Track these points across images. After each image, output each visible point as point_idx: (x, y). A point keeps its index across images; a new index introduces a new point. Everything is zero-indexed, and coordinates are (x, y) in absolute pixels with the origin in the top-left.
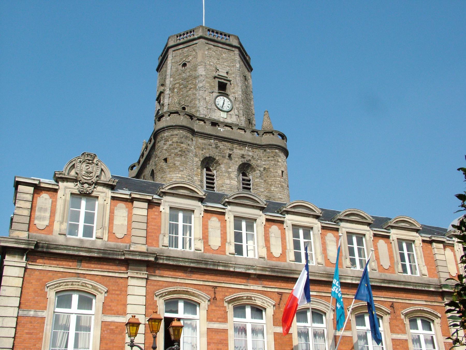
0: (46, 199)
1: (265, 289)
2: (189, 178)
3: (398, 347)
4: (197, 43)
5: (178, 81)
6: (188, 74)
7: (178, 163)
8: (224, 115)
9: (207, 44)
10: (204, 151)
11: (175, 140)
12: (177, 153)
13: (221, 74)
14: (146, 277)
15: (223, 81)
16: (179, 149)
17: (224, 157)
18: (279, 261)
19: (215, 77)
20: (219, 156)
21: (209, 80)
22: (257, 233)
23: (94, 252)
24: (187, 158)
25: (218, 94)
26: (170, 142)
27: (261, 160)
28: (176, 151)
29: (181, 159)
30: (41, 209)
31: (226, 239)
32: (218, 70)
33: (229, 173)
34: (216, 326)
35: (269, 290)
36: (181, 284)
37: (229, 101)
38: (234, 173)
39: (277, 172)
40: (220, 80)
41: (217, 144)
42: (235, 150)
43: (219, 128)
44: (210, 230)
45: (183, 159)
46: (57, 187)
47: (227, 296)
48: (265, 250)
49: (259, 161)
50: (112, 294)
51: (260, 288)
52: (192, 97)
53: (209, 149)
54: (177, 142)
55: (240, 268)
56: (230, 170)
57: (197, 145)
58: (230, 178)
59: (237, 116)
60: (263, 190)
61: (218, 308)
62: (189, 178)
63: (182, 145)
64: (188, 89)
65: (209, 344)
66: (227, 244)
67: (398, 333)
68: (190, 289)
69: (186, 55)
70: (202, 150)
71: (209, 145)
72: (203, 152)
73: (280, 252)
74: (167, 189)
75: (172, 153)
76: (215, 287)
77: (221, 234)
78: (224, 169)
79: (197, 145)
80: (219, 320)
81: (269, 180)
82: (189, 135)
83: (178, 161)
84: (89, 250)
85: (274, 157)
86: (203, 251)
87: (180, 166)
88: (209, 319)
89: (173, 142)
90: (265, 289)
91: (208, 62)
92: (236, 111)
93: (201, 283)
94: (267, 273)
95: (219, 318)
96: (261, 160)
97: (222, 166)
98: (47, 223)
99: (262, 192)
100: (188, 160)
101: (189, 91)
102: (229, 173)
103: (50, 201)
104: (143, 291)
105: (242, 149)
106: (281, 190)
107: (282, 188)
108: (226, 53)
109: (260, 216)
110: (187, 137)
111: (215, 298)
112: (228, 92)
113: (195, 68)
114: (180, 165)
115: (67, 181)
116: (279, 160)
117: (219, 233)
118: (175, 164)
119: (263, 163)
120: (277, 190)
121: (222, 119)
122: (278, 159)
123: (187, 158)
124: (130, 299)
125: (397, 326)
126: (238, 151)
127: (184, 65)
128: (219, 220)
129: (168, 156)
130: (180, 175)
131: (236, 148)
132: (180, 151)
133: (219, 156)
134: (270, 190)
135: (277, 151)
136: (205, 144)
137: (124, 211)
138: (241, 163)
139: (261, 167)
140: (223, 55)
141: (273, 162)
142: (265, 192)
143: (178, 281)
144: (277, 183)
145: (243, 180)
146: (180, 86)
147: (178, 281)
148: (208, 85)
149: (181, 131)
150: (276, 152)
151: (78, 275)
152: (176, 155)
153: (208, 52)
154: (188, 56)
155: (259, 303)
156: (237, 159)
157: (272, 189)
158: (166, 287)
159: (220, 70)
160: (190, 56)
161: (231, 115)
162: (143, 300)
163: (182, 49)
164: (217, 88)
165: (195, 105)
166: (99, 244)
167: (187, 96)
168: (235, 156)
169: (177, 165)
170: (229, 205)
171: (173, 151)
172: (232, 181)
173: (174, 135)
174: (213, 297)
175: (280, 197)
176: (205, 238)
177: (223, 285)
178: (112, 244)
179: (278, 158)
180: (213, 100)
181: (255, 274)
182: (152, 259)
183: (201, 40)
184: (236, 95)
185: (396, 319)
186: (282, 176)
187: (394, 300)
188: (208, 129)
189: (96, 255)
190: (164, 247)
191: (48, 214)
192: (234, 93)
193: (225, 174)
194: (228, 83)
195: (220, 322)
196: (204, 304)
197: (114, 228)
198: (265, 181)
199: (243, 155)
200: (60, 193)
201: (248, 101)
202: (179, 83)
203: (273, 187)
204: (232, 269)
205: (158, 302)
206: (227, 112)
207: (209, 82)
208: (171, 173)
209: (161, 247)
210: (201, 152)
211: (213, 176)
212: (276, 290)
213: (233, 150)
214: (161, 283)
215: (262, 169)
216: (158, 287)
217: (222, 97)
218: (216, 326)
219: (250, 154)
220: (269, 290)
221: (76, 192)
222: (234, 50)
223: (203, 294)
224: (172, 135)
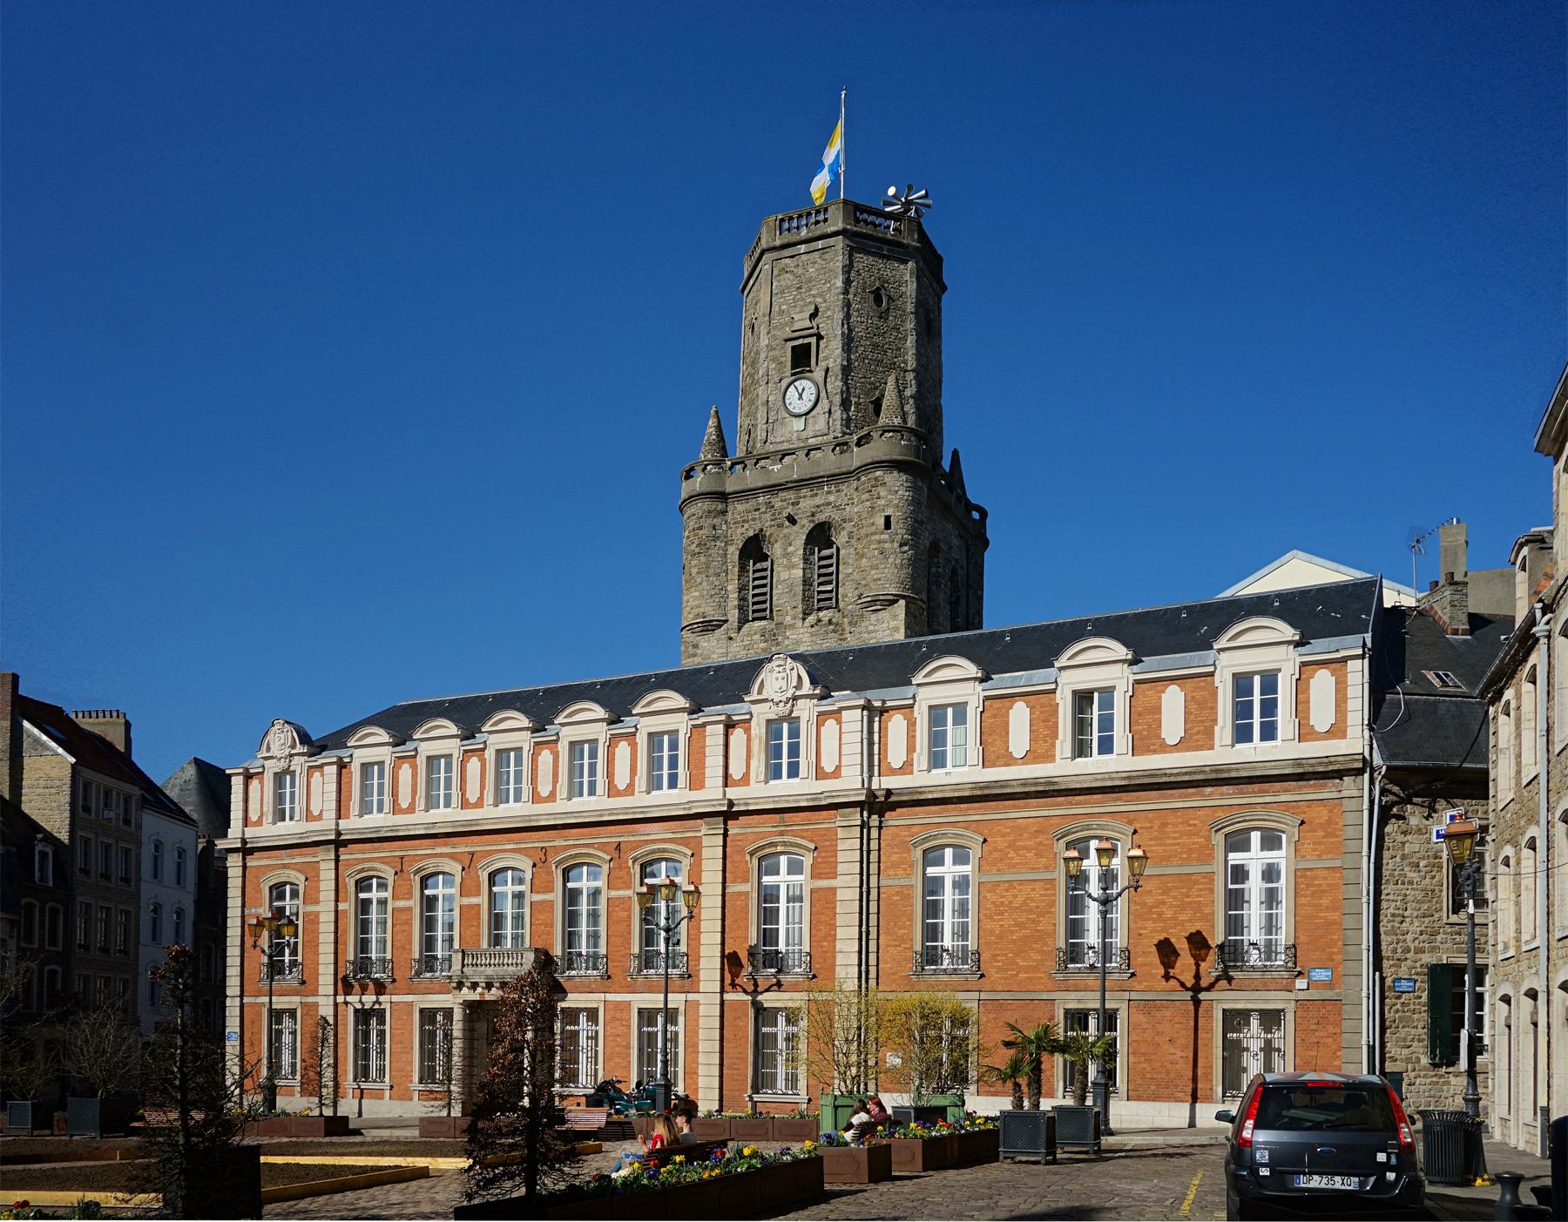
8: (798, 424)
10: (746, 526)
24: (710, 555)
54: (694, 530)
56: (790, 549)
60: (850, 571)
67: (619, 889)
70: (743, 526)
71: (755, 510)
76: (402, 858)
96: (853, 503)
105: (816, 495)
114: (697, 573)
122: (878, 494)
125: (621, 878)
126: (807, 504)
130: (697, 594)
131: (805, 497)
133: (771, 526)
135: (878, 473)
144: (872, 547)
150: (876, 479)
151: (285, 866)
175: (876, 577)
179: (879, 489)
185: (620, 868)
187: (622, 839)
223: (388, 868)
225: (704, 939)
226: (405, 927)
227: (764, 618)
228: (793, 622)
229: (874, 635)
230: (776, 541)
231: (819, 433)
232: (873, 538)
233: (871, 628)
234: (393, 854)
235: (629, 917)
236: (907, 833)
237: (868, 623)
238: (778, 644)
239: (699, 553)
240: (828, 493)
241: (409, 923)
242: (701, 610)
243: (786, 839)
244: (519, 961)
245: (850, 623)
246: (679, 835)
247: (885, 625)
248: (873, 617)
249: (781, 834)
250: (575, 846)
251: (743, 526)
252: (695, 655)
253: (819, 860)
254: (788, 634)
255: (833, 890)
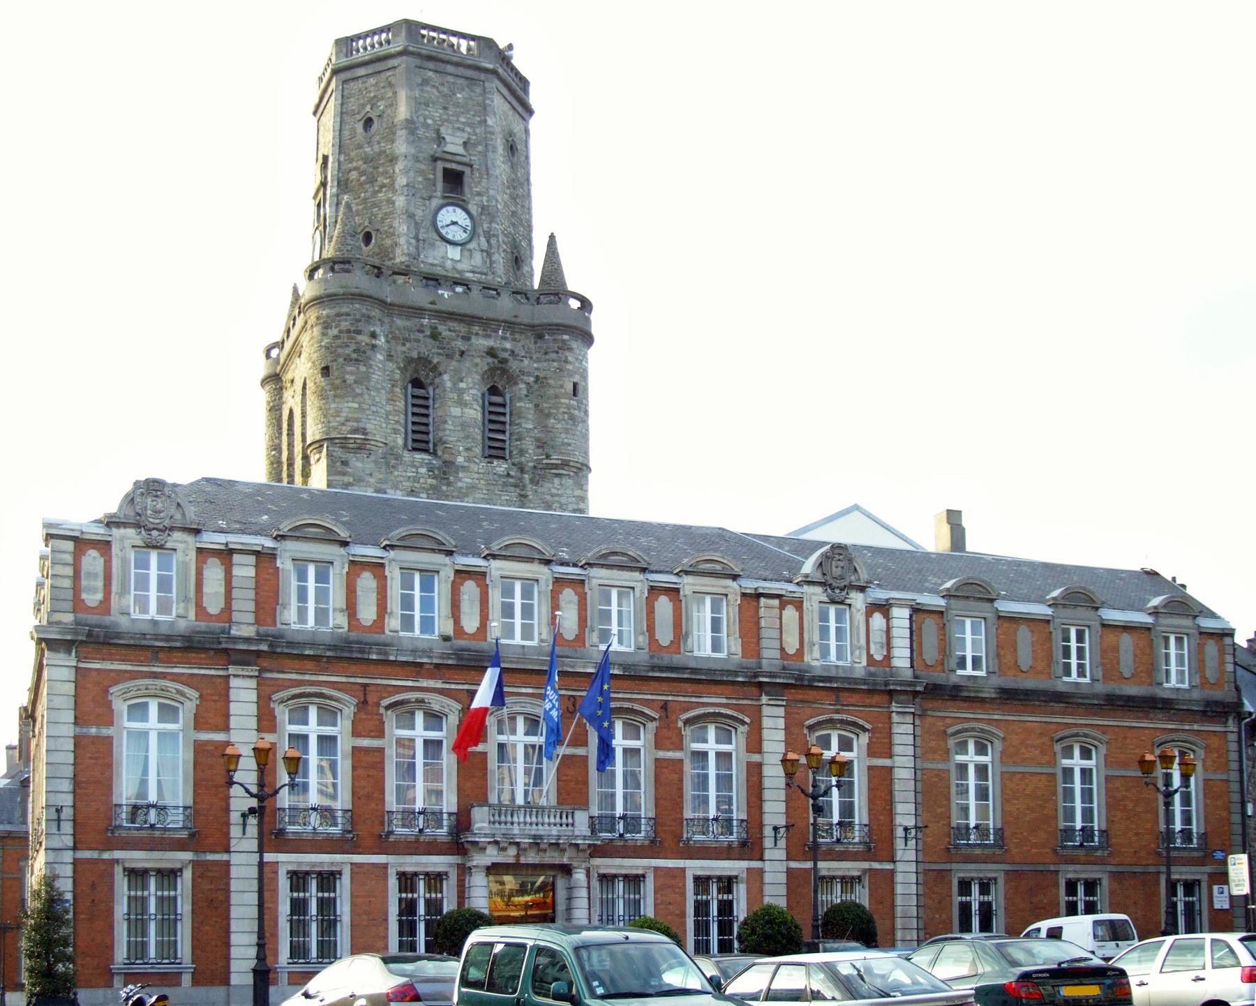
0: (95, 558)
1: (447, 686)
2: (374, 409)
3: (664, 770)
4: (394, 68)
5: (355, 164)
6: (376, 148)
7: (350, 379)
8: (454, 253)
9: (420, 67)
10: (408, 345)
11: (345, 325)
12: (349, 355)
13: (450, 148)
14: (257, 674)
15: (454, 166)
16: (353, 347)
17: (449, 356)
18: (474, 639)
19: (435, 159)
20: (440, 354)
21: (423, 167)
22: (439, 594)
23: (176, 641)
25: (441, 201)
26: (335, 332)
27: (531, 358)
28: (347, 351)
29: (358, 368)
30: (89, 574)
31: (386, 608)
32: (444, 138)
33: (461, 392)
34: (365, 742)
35: (453, 686)
36: (312, 683)
37: (466, 216)
38: (471, 391)
39: (562, 387)
40: (449, 166)
41: (436, 328)
42: (474, 340)
43: (440, 292)
44: (359, 593)
45: (363, 369)
46: (109, 539)
47: (384, 698)
48: (451, 622)
49: (526, 362)
50: (207, 701)
51: (438, 684)
52: (385, 209)
53: (418, 341)
54: (348, 331)
55: (405, 656)
56: (462, 385)
57: (392, 332)
58: (462, 404)
59: (485, 254)
60: (531, 426)
61: (370, 717)
62: (374, 409)
63: (360, 337)
64: (377, 188)
65: (354, 768)
66: (387, 616)
67: (668, 750)
68: (325, 691)
69: (372, 95)
70: (404, 345)
71: (419, 331)
72: (404, 349)
73: (477, 625)
74: (286, 530)
75: (339, 356)
76: (365, 686)
77: (378, 599)
78: (449, 384)
79: (392, 332)
80: (373, 734)
81: (545, 405)
82: (376, 313)
83: (352, 373)
84: (168, 638)
85: (557, 352)
86: (346, 629)
87: (355, 386)
88: (356, 733)
89: (341, 332)
90: (447, 686)
91: (421, 119)
92: (483, 240)
93: (343, 679)
94: (450, 662)
95: (371, 731)
97: (446, 377)
98: (99, 596)
99: (529, 430)
100: (371, 371)
101: (381, 192)
102: (461, 392)
103: (102, 560)
104: (253, 696)
106: (569, 427)
107: (570, 422)
108: (463, 90)
109: (445, 565)
110: (369, 317)
111: (365, 702)
112: (468, 195)
113: (390, 135)
114: (356, 382)
115: (125, 527)
116: (570, 358)
117: (373, 597)
118: (345, 381)
119: (535, 365)
120: (559, 426)
121: (449, 262)
122: (566, 357)
123: (371, 366)
124: (234, 708)
125: (668, 738)
126: (482, 343)
127: (368, 122)
128: (375, 577)
129: (332, 361)
130: (356, 405)
131: (477, 334)
132: (354, 351)
133: (440, 354)
134: (546, 426)
135: (566, 337)
136: (410, 330)
137: (219, 570)
138: (486, 368)
139: (529, 374)
140: (459, 95)
141: (555, 364)
142: (536, 431)
143: (307, 677)
144: (562, 410)
145: (491, 404)
146: (361, 176)
147: (307, 677)
148: (420, 179)
149: (357, 306)
150: (563, 341)
152: (348, 359)
153: (422, 91)
154: (373, 102)
155: (436, 707)
156: (478, 360)
157: (550, 425)
158: (289, 687)
159: (448, 138)
160: (382, 99)
161: (470, 250)
162: (253, 709)
163: (365, 79)
164: (440, 185)
165: (391, 230)
166: (182, 626)
167: (375, 205)
168: (474, 353)
169: (348, 382)
170: (393, 550)
171: (340, 350)
172: (466, 410)
173: (342, 315)
174: (362, 699)
175: (566, 441)
176: (351, 608)
177: (379, 681)
178: (202, 626)
180: (430, 217)
181: (431, 664)
182: (264, 647)
183: (404, 58)
184: (485, 198)
185: (668, 728)
186: (575, 394)
188: (417, 294)
189: (178, 644)
190: (284, 627)
191: (100, 583)
192: (479, 194)
193: (451, 395)
194: (467, 170)
195: (372, 737)
196: (349, 711)
197: (204, 599)
198: (536, 406)
199: (492, 348)
200: (115, 549)
201: (516, 204)
202: (356, 169)
203: (552, 421)
204: (392, 658)
205: (276, 710)
206: (462, 245)
207: (421, 172)
208: (337, 400)
209: (279, 625)
210: (400, 348)
211: (427, 398)
212: (466, 687)
213: (469, 339)
214: (280, 682)
215: (532, 379)
216: (276, 688)
217: (450, 209)
218: (365, 742)
219: (508, 345)
220: (453, 686)
221: (140, 543)
222: (482, 78)
223: (346, 697)
224: (338, 315)
225: (767, 807)
226: (372, 772)
227: (426, 451)
228: (466, 464)
229: (556, 499)
230: (445, 372)
231: (476, 269)
232: (563, 401)
233: (554, 491)
234: (352, 680)
235: (681, 780)
236: (941, 724)
237: (550, 485)
238: (449, 484)
239: (357, 360)
240: (504, 338)
241: (380, 766)
242: (361, 425)
243: (844, 717)
244: (570, 820)
245: (532, 481)
246: (734, 702)
247: (569, 492)
248: (556, 481)
249: (837, 712)
250: (312, 683)
251: (404, 345)
252: (344, 474)
253: (874, 740)
254: (461, 475)
255: (890, 770)
